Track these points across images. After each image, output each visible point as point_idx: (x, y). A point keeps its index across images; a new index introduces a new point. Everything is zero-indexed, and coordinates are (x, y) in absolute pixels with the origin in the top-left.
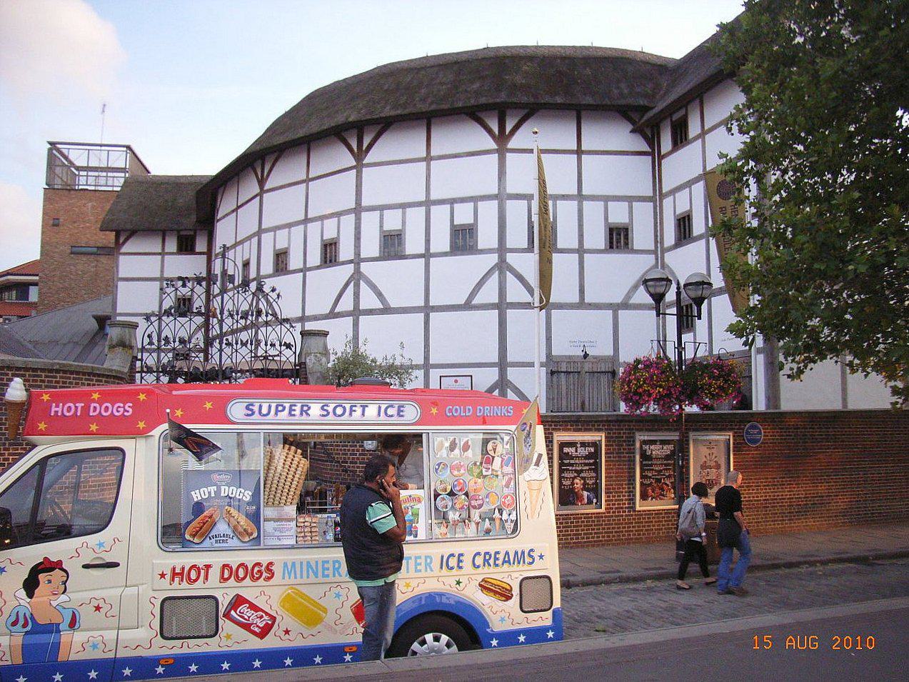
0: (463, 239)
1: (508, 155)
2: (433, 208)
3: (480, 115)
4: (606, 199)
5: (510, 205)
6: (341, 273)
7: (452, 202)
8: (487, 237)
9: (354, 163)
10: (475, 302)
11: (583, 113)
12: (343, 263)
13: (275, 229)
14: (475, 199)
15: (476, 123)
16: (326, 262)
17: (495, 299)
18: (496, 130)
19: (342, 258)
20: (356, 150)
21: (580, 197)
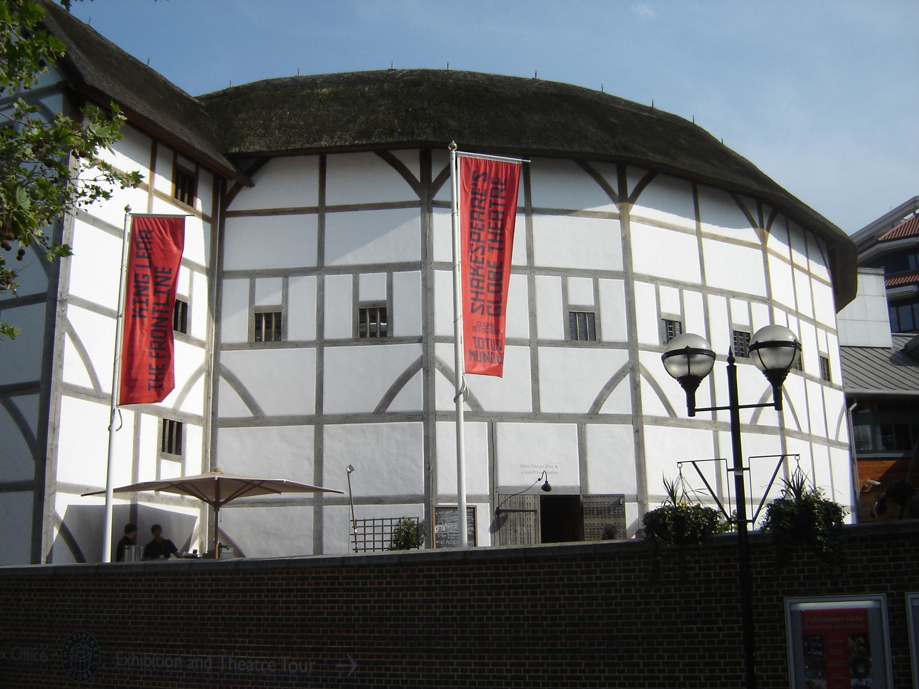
0: (583, 327)
1: (634, 226)
2: (540, 279)
3: (594, 165)
4: (731, 295)
5: (638, 285)
6: (396, 358)
7: (565, 273)
8: (612, 326)
9: (415, 197)
10: (601, 412)
11: (699, 187)
12: (400, 340)
13: (252, 275)
14: (596, 275)
15: (590, 177)
16: (363, 335)
17: (628, 410)
18: (615, 188)
19: (398, 331)
20: (418, 177)
21: (703, 289)
